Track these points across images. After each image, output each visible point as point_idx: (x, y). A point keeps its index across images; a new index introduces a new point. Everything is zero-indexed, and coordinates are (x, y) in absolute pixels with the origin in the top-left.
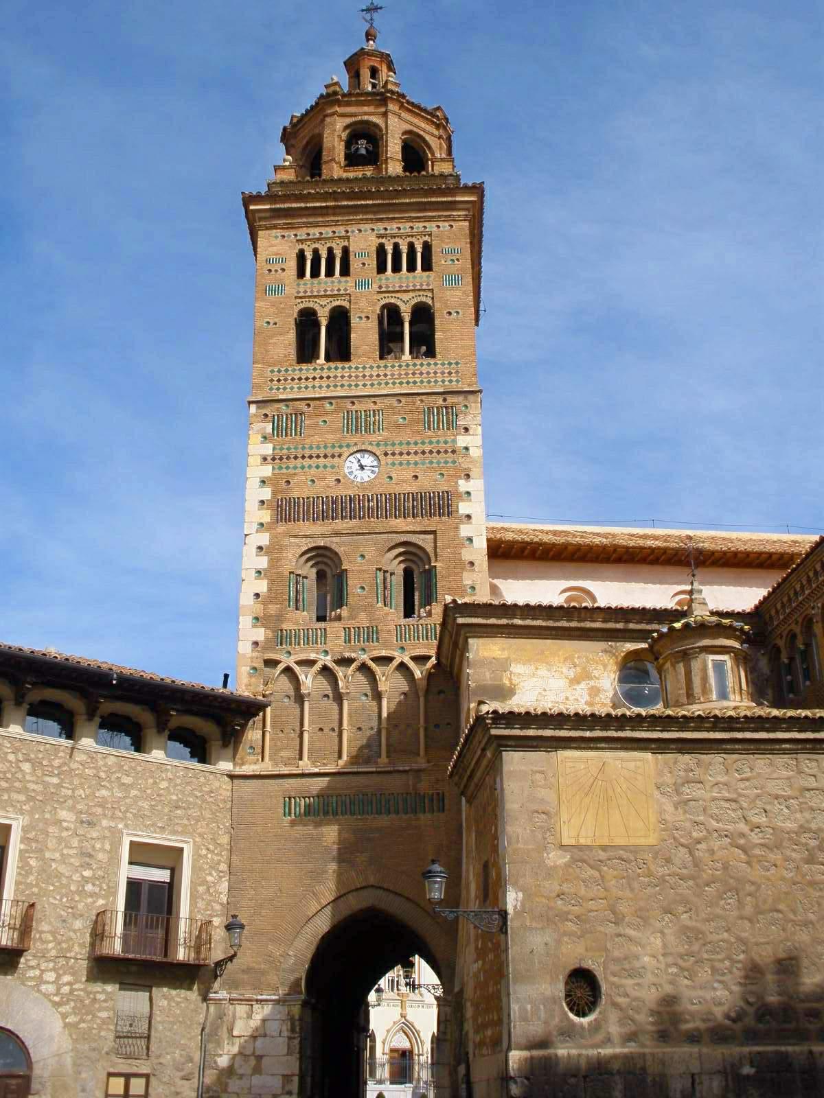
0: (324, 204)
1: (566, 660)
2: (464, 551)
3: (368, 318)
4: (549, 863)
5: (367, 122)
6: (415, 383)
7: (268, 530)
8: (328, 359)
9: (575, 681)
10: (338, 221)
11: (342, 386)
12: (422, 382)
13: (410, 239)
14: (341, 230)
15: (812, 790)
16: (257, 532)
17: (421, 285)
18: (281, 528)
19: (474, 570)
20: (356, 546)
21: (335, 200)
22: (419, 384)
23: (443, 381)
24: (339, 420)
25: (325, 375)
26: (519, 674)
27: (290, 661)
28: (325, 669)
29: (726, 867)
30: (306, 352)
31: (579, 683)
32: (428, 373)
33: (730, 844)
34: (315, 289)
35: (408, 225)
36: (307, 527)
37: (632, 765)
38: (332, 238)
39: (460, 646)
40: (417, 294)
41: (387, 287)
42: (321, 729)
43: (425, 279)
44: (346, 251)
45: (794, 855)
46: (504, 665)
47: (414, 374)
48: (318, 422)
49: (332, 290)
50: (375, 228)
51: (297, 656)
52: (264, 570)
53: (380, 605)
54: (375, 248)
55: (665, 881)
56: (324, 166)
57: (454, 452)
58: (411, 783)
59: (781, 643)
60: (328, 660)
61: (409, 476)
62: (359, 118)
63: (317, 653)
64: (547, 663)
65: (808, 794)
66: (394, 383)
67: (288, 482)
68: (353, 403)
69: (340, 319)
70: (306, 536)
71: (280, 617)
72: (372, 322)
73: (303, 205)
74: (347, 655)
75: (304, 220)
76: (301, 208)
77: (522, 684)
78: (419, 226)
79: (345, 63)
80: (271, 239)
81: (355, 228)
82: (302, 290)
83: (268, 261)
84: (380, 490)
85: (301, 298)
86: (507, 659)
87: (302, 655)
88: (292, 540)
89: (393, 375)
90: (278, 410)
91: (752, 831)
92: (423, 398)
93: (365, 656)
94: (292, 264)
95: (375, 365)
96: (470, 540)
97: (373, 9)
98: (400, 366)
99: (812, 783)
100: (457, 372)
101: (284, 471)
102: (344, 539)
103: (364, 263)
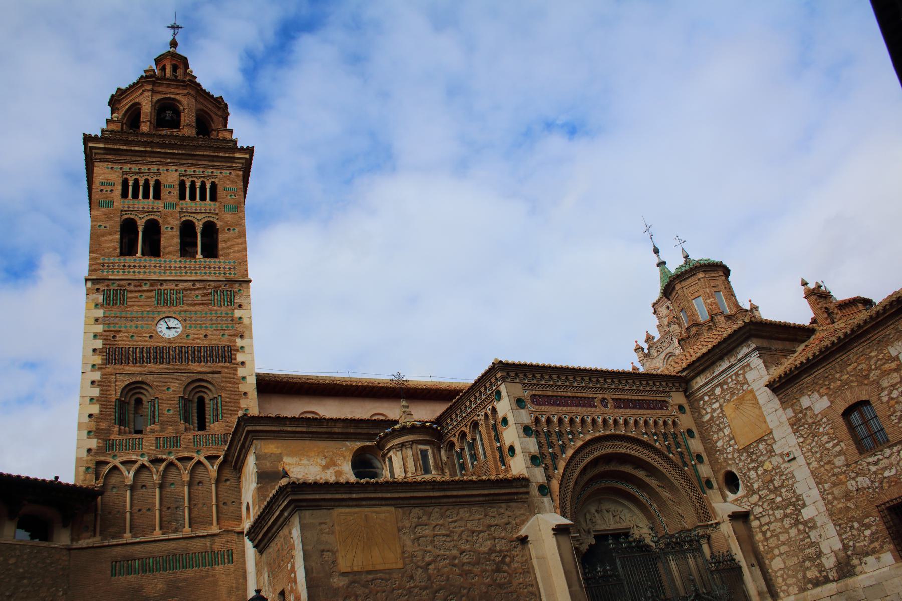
0: (143, 149)
1: (319, 453)
2: (240, 385)
3: (172, 228)
4: (335, 586)
5: (174, 99)
6: (205, 273)
7: (99, 369)
8: (143, 254)
9: (326, 467)
10: (153, 161)
11: (155, 273)
12: (210, 273)
13: (202, 179)
14: (154, 169)
15: (494, 526)
16: (92, 370)
17: (210, 210)
18: (110, 368)
19: (247, 398)
20: (165, 381)
21: (152, 147)
22: (208, 275)
23: (225, 274)
24: (153, 295)
25: (142, 265)
26: (289, 464)
27: (117, 462)
28: (143, 466)
29: (448, 579)
30: (127, 248)
31: (328, 468)
32: (215, 268)
33: (449, 564)
34: (136, 206)
35: (201, 170)
36: (129, 368)
37: (383, 516)
38: (149, 173)
39: (246, 446)
41: (187, 209)
42: (140, 510)
43: (213, 206)
44: (158, 184)
45: (487, 567)
46: (279, 458)
47: (205, 268)
48: (137, 296)
49: (148, 208)
50: (179, 170)
51: (122, 458)
52: (97, 397)
53: (182, 422)
54: (178, 183)
55: (410, 591)
56: (143, 124)
57: (232, 320)
58: (208, 544)
59: (455, 440)
60: (145, 460)
61: (203, 336)
62: (168, 96)
63: (137, 456)
64: (307, 456)
65: (492, 529)
66: (191, 273)
67: (114, 337)
68: (161, 285)
69: (153, 229)
70: (129, 374)
71: (109, 431)
72: (176, 232)
73: (129, 148)
74: (159, 456)
75: (128, 158)
76: (127, 150)
77: (291, 470)
78: (208, 172)
79: (155, 59)
80: (104, 168)
81: (163, 169)
82: (126, 206)
83: (102, 184)
84: (183, 344)
85: (125, 211)
86: (280, 454)
87: (125, 458)
88: (118, 377)
89: (190, 267)
90: (108, 286)
91: (460, 555)
92: (212, 284)
93: (173, 457)
94: (119, 187)
95: (178, 260)
96: (244, 378)
97: (175, 27)
98: (196, 262)
99: (493, 522)
100: (234, 268)
101: (113, 329)
102: (156, 376)
103: (170, 194)
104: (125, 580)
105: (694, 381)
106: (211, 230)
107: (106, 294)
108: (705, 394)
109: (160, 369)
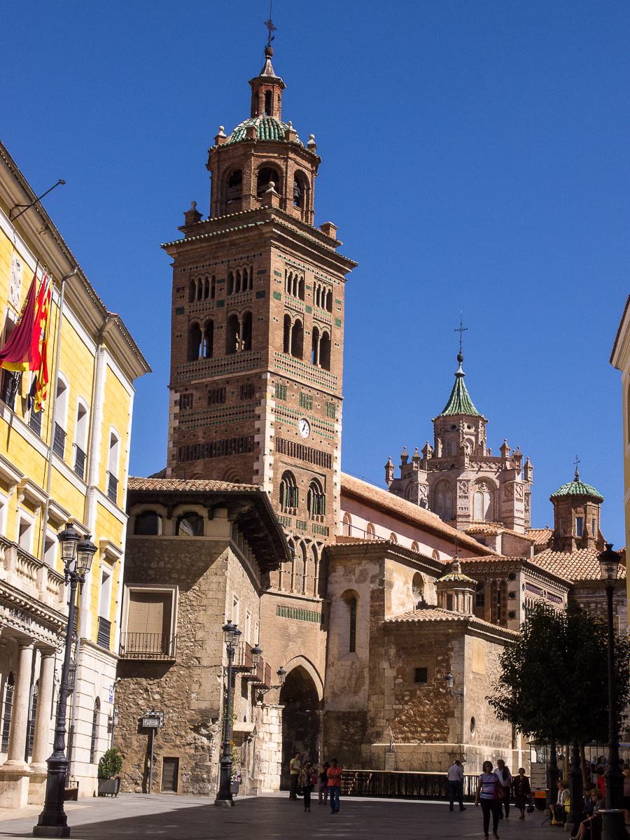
7: (273, 455)
16: (270, 455)
18: (278, 455)
20: (301, 475)
36: (286, 458)
39: (367, 555)
40: (327, 326)
44: (302, 282)
62: (301, 168)
67: (280, 428)
70: (285, 463)
81: (307, 266)
83: (275, 272)
85: (286, 306)
92: (326, 395)
101: (279, 420)
104: (282, 619)
105: (578, 590)
106: (326, 340)
107: (277, 386)
108: (582, 603)
109: (300, 464)
